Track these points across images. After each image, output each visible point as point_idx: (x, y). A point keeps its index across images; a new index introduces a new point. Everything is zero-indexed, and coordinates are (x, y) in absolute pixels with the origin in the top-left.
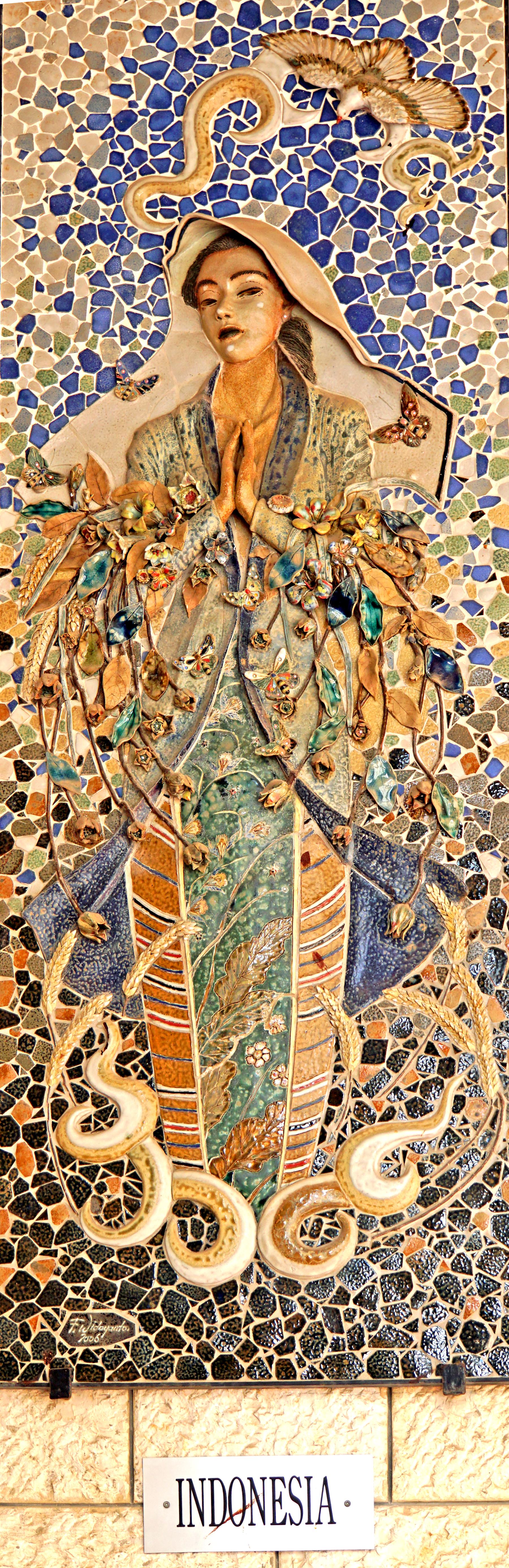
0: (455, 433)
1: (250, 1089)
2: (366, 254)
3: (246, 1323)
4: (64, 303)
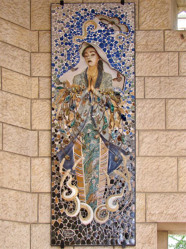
0: (126, 80)
1: (93, 188)
2: (112, 51)
3: (92, 232)
4: (62, 55)
